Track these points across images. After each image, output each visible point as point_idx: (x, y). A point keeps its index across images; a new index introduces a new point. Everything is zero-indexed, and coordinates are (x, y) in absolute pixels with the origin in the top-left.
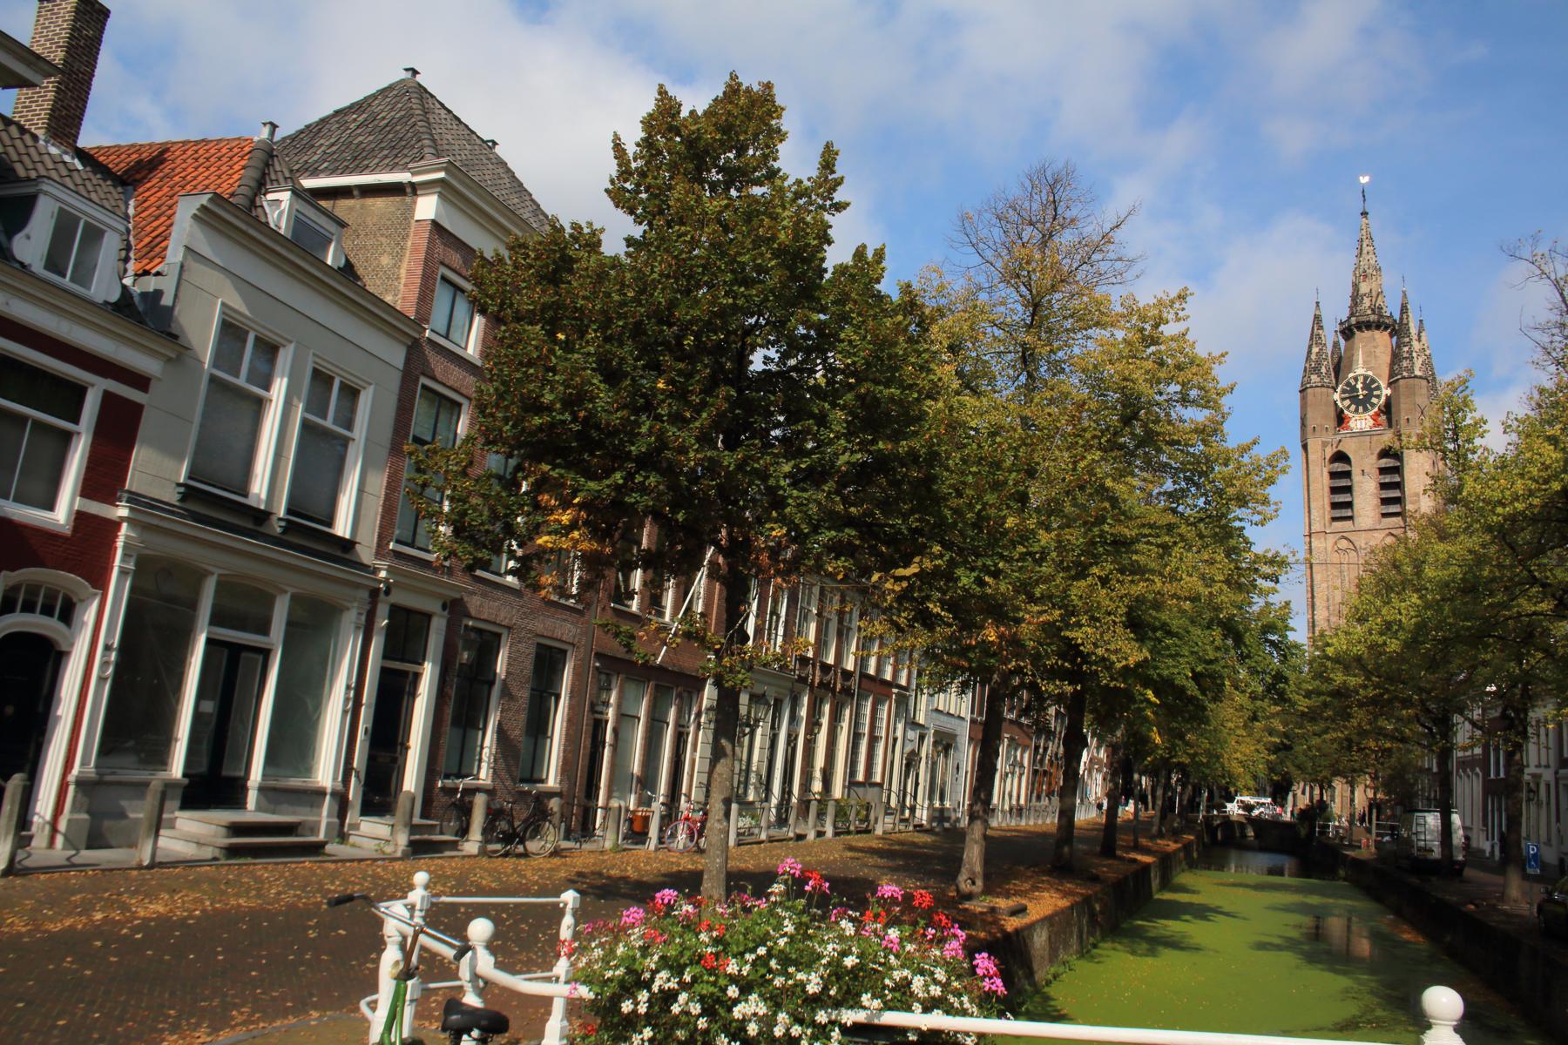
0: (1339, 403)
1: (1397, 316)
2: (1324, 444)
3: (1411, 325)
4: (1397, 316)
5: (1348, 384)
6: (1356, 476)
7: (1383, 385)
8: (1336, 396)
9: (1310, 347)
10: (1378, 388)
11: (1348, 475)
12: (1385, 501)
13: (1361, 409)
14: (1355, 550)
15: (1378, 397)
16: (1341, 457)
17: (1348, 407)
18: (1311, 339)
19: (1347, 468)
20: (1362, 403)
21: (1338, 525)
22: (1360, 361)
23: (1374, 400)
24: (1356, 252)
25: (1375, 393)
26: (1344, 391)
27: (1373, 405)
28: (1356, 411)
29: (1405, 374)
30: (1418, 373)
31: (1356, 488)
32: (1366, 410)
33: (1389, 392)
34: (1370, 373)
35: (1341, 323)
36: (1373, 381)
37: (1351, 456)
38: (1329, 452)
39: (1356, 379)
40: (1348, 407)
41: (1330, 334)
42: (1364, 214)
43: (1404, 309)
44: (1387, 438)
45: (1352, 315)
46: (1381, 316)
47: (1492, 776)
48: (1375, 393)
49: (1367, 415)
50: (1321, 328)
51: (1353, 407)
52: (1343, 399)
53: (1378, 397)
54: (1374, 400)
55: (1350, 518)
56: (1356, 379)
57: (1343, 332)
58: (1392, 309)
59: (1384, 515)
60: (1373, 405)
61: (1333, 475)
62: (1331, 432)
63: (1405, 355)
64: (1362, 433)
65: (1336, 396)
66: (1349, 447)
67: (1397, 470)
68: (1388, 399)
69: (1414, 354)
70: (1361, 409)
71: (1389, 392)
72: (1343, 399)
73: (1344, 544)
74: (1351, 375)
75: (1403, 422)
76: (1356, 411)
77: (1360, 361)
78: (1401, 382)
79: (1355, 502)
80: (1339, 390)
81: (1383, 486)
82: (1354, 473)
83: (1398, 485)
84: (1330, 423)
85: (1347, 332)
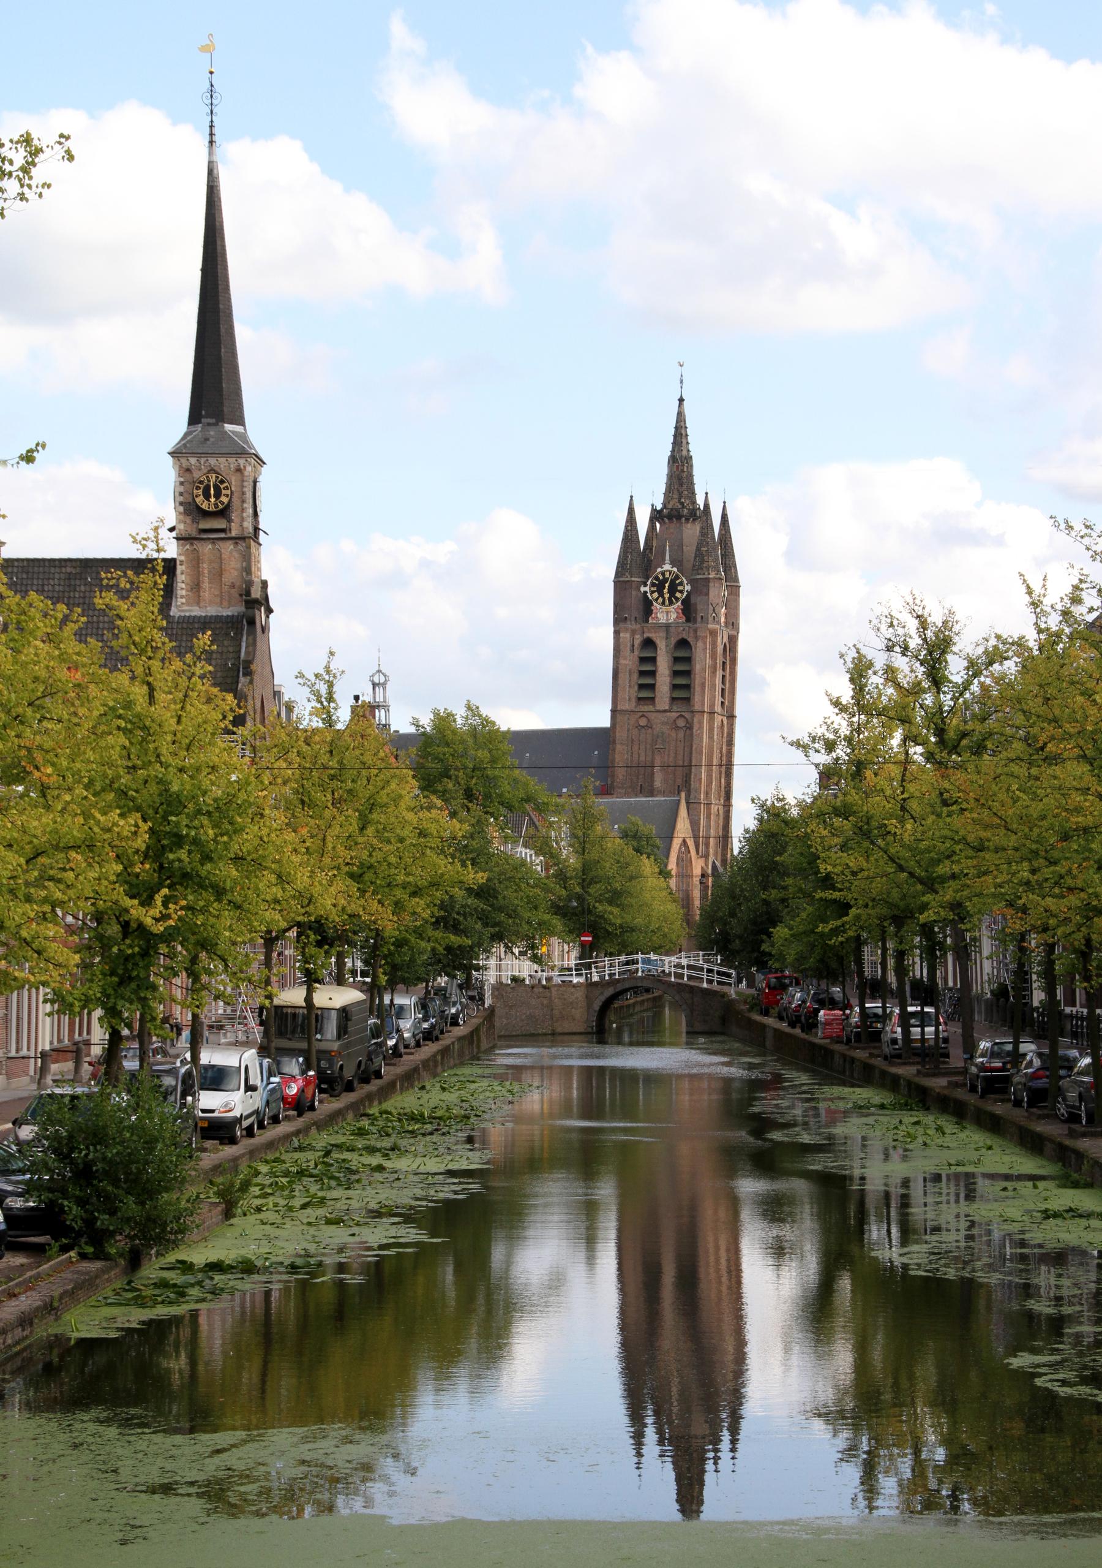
5: (657, 578)
10: (681, 584)
16: (649, 643)
17: (657, 600)
22: (667, 557)
23: (678, 595)
24: (671, 439)
25: (680, 588)
26: (653, 585)
32: (671, 603)
33: (688, 588)
35: (654, 510)
39: (663, 574)
40: (657, 600)
42: (681, 400)
43: (707, 506)
45: (665, 505)
48: (680, 588)
49: (671, 608)
53: (681, 592)
54: (678, 595)
56: (663, 574)
58: (700, 501)
60: (677, 599)
66: (652, 635)
68: (689, 594)
71: (688, 588)
72: (652, 592)
74: (659, 570)
75: (699, 619)
77: (667, 557)
79: (658, 684)
82: (658, 659)
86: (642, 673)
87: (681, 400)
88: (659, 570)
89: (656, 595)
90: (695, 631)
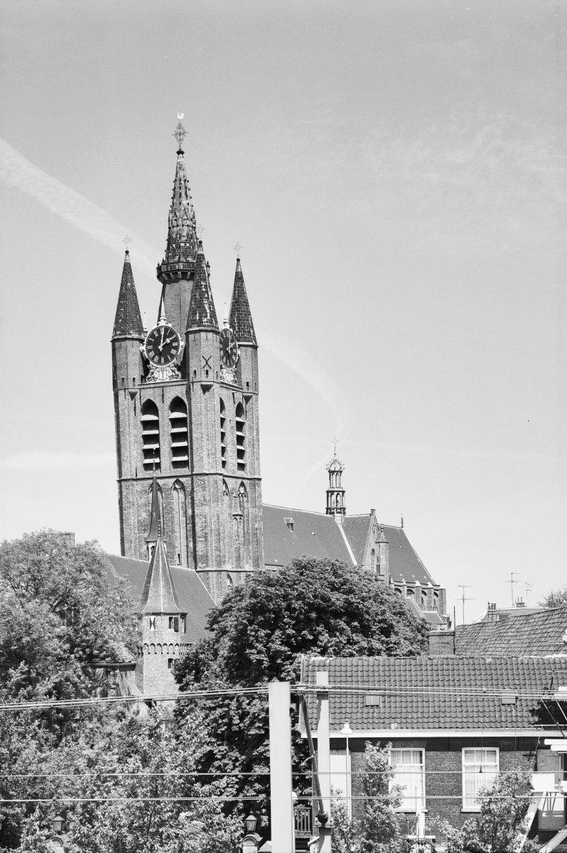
0: (145, 353)
7: (180, 338)
13: (163, 359)
15: (176, 348)
21: (149, 474)
27: (173, 356)
28: (159, 363)
32: (167, 361)
34: (170, 325)
40: (153, 359)
51: (157, 359)
52: (149, 351)
54: (173, 352)
60: (173, 356)
62: (138, 382)
70: (163, 359)
89: (152, 354)
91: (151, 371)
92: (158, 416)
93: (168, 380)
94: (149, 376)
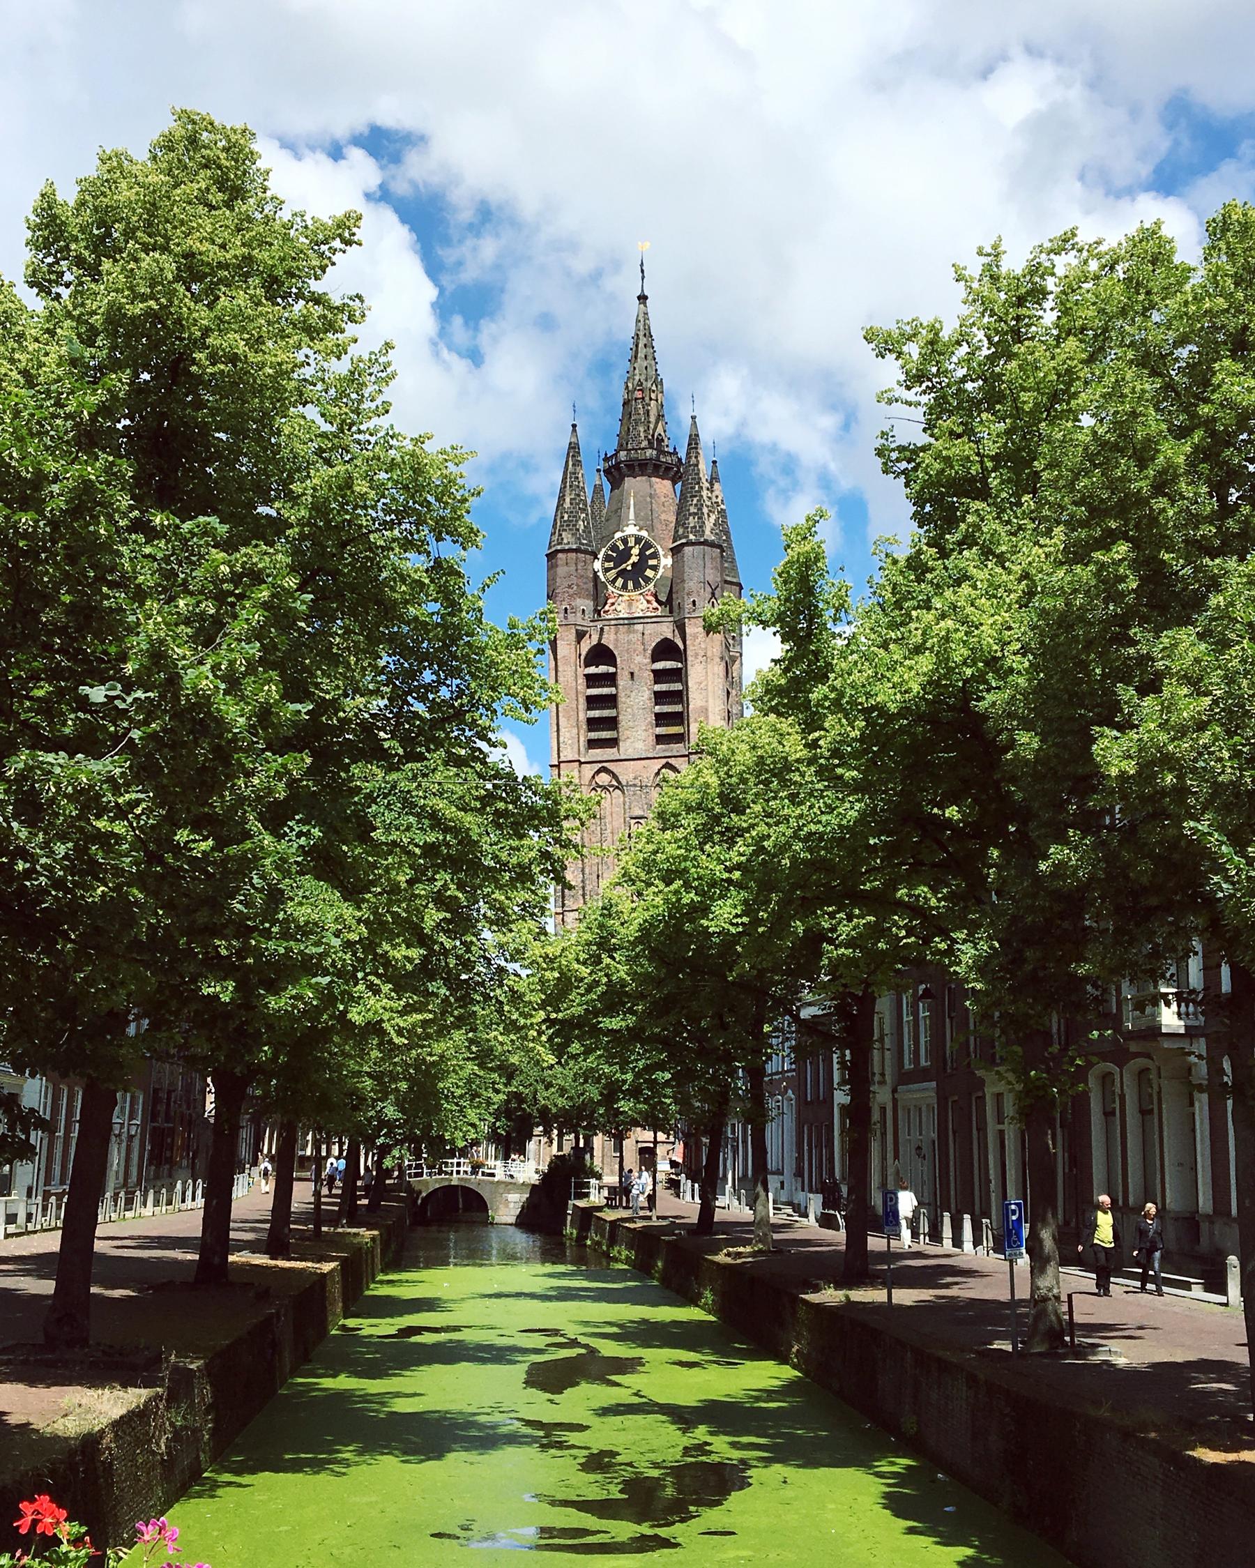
0: (600, 574)
1: (682, 454)
2: (580, 636)
3: (702, 466)
4: (682, 454)
5: (614, 548)
6: (623, 680)
7: (661, 552)
8: (597, 565)
9: (562, 490)
10: (655, 555)
11: (611, 679)
12: (661, 719)
13: (630, 585)
14: (620, 787)
15: (655, 568)
16: (601, 654)
18: (564, 481)
19: (612, 670)
20: (635, 576)
21: (598, 754)
24: (630, 354)
25: (651, 562)
26: (607, 558)
28: (624, 587)
29: (692, 537)
30: (709, 535)
31: (622, 698)
32: (637, 586)
34: (644, 533)
35: (606, 459)
36: (648, 545)
37: (616, 653)
38: (586, 646)
39: (624, 541)
41: (591, 477)
42: (643, 298)
43: (694, 441)
44: (666, 630)
45: (621, 447)
46: (661, 452)
47: (907, 1066)
48: (651, 562)
50: (577, 463)
51: (620, 582)
52: (607, 570)
53: (655, 568)
54: (649, 573)
55: (613, 743)
57: (607, 472)
59: (660, 739)
60: (647, 580)
61: (592, 680)
63: (693, 510)
64: (631, 621)
65: (597, 565)
66: (609, 640)
67: (678, 675)
69: (705, 510)
70: (630, 585)
72: (607, 570)
73: (604, 779)
74: (618, 535)
75: (688, 606)
76: (624, 587)
78: (688, 549)
80: (601, 556)
81: (660, 697)
82: (619, 677)
83: (679, 697)
84: (586, 604)
85: (616, 472)
86: (592, 702)
87: (643, 298)
88: (618, 535)
90: (681, 627)
91: (610, 601)
92: (615, 666)
93: (641, 614)
94: (607, 608)
